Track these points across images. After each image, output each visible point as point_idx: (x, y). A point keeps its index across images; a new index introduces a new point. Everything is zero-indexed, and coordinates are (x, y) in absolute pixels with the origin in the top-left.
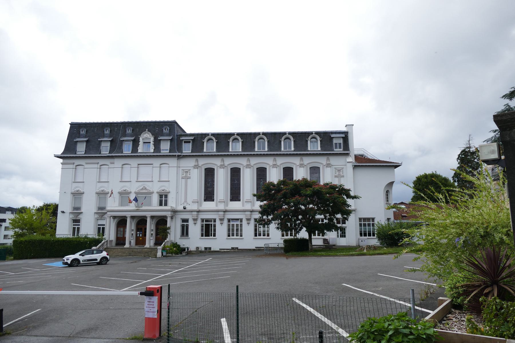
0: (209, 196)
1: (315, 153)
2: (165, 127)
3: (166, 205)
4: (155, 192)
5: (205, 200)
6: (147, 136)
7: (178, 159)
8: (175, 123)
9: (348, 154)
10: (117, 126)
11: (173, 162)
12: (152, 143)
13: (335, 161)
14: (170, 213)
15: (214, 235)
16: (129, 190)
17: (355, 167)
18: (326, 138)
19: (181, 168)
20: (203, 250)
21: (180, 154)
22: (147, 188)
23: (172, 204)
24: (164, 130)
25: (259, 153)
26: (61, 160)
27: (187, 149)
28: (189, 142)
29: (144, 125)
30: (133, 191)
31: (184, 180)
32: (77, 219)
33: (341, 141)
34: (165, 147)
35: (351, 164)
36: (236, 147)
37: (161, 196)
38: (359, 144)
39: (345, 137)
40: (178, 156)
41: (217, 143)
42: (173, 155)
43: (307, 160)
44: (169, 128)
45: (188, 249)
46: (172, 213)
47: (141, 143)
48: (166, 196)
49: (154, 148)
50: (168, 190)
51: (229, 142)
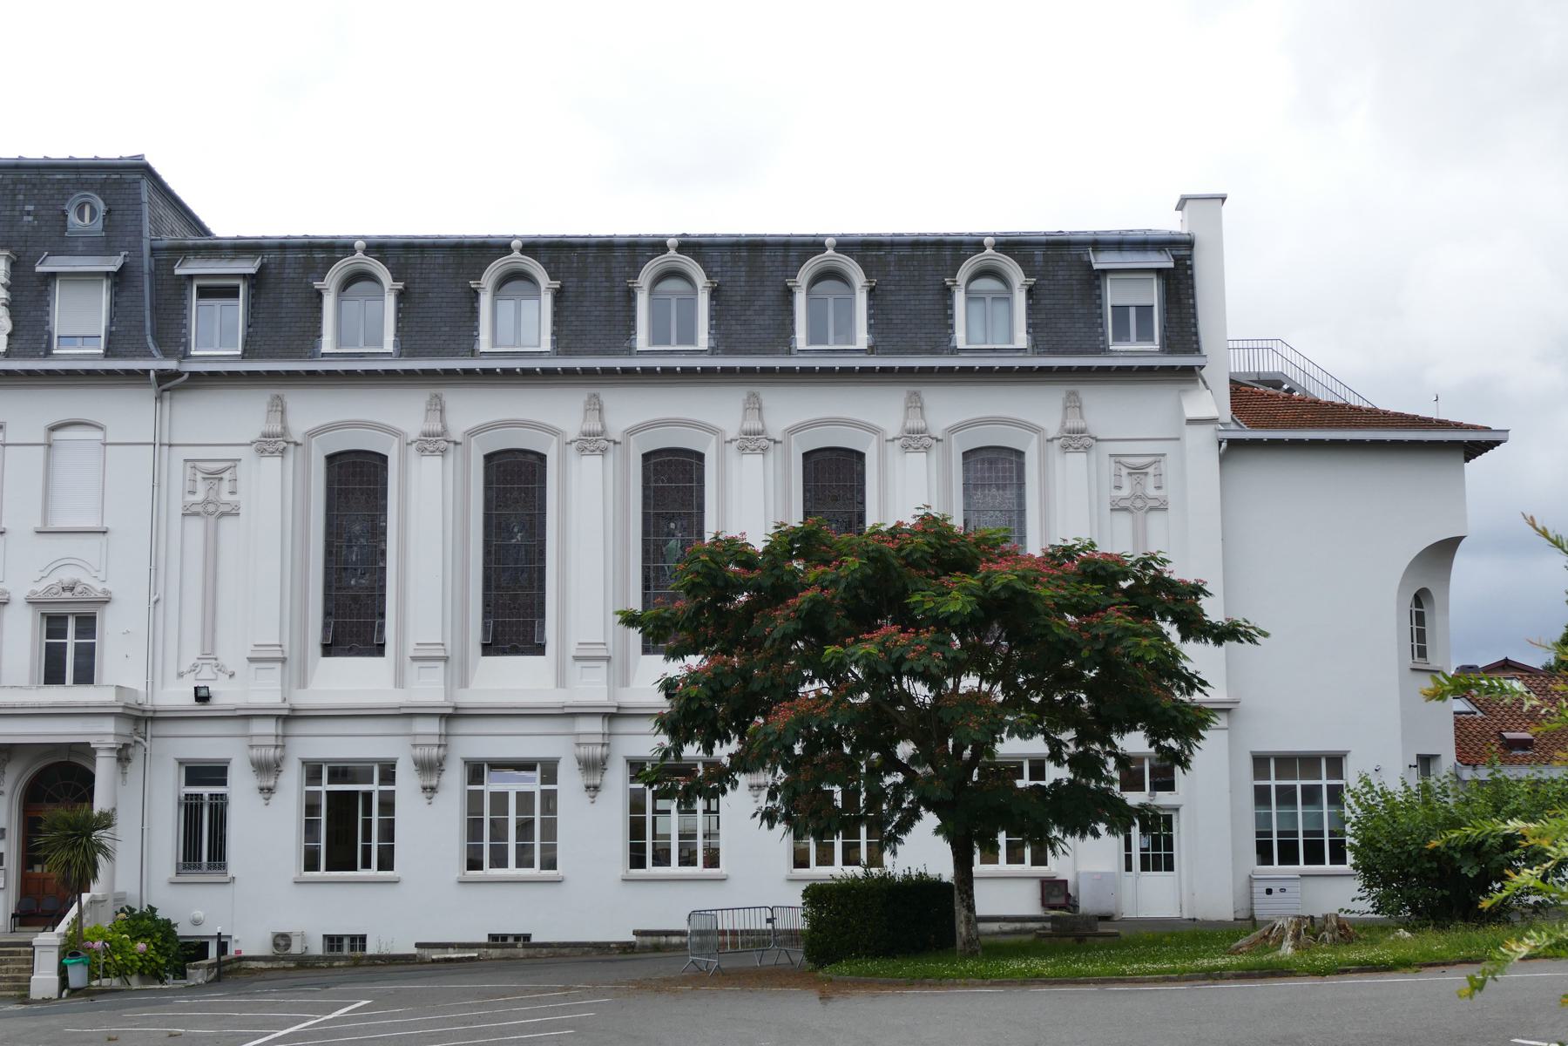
0: (353, 621)
1: (996, 363)
2: (77, 198)
3: (85, 675)
4: (19, 594)
5: (328, 650)
7: (159, 398)
8: (141, 170)
9: (1189, 374)
11: (129, 414)
13: (1116, 414)
14: (109, 726)
15: (386, 863)
18: (1062, 271)
19: (180, 454)
20: (317, 948)
21: (171, 365)
23: (122, 668)
24: (73, 217)
25: (658, 363)
27: (217, 331)
28: (232, 293)
31: (196, 527)
33: (1151, 294)
35: (1207, 432)
36: (520, 324)
37: (54, 625)
38: (1260, 314)
39: (1176, 268)
40: (164, 377)
41: (401, 296)
42: (130, 373)
43: (953, 412)
44: (101, 206)
45: (222, 948)
46: (127, 728)
48: (87, 625)
50: (97, 589)
51: (475, 295)
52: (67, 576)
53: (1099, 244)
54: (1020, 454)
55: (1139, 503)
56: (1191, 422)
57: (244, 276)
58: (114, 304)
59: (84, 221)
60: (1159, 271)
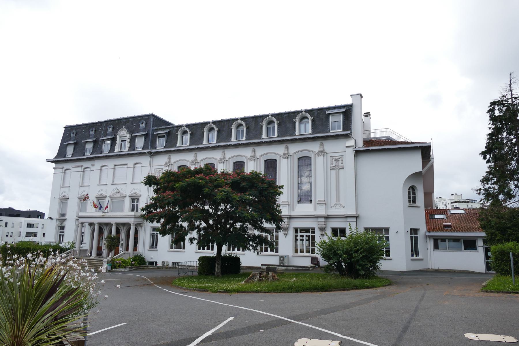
2: (141, 122)
6: (123, 134)
7: (151, 157)
8: (153, 115)
9: (347, 136)
10: (101, 125)
12: (128, 140)
13: (333, 147)
14: (133, 219)
15: (184, 248)
16: (139, 193)
17: (358, 153)
19: (154, 168)
20: (171, 265)
22: (121, 191)
25: (236, 143)
26: (53, 165)
27: (161, 144)
29: (124, 122)
30: (108, 195)
32: (62, 225)
33: (341, 118)
34: (140, 143)
35: (351, 149)
37: (133, 200)
40: (150, 153)
43: (294, 149)
44: (144, 122)
45: (156, 263)
47: (118, 142)
49: (129, 145)
52: (134, 192)
53: (329, 108)
54: (310, 158)
55: (337, 167)
56: (347, 147)
57: (166, 133)
58: (145, 141)
59: (143, 126)
60: (342, 112)
